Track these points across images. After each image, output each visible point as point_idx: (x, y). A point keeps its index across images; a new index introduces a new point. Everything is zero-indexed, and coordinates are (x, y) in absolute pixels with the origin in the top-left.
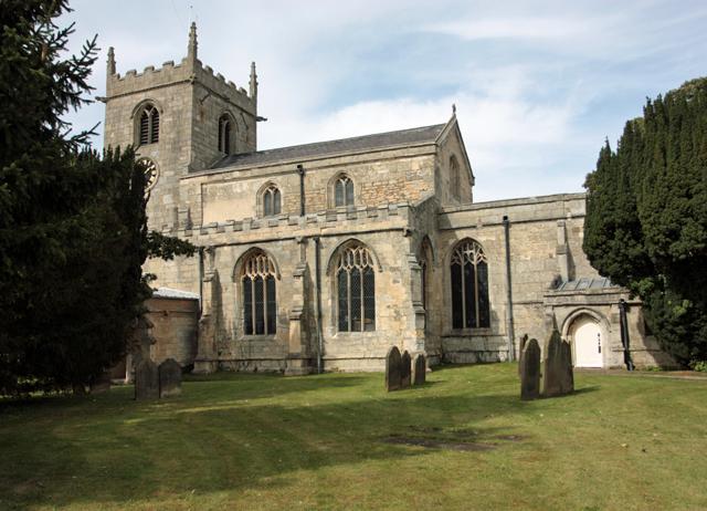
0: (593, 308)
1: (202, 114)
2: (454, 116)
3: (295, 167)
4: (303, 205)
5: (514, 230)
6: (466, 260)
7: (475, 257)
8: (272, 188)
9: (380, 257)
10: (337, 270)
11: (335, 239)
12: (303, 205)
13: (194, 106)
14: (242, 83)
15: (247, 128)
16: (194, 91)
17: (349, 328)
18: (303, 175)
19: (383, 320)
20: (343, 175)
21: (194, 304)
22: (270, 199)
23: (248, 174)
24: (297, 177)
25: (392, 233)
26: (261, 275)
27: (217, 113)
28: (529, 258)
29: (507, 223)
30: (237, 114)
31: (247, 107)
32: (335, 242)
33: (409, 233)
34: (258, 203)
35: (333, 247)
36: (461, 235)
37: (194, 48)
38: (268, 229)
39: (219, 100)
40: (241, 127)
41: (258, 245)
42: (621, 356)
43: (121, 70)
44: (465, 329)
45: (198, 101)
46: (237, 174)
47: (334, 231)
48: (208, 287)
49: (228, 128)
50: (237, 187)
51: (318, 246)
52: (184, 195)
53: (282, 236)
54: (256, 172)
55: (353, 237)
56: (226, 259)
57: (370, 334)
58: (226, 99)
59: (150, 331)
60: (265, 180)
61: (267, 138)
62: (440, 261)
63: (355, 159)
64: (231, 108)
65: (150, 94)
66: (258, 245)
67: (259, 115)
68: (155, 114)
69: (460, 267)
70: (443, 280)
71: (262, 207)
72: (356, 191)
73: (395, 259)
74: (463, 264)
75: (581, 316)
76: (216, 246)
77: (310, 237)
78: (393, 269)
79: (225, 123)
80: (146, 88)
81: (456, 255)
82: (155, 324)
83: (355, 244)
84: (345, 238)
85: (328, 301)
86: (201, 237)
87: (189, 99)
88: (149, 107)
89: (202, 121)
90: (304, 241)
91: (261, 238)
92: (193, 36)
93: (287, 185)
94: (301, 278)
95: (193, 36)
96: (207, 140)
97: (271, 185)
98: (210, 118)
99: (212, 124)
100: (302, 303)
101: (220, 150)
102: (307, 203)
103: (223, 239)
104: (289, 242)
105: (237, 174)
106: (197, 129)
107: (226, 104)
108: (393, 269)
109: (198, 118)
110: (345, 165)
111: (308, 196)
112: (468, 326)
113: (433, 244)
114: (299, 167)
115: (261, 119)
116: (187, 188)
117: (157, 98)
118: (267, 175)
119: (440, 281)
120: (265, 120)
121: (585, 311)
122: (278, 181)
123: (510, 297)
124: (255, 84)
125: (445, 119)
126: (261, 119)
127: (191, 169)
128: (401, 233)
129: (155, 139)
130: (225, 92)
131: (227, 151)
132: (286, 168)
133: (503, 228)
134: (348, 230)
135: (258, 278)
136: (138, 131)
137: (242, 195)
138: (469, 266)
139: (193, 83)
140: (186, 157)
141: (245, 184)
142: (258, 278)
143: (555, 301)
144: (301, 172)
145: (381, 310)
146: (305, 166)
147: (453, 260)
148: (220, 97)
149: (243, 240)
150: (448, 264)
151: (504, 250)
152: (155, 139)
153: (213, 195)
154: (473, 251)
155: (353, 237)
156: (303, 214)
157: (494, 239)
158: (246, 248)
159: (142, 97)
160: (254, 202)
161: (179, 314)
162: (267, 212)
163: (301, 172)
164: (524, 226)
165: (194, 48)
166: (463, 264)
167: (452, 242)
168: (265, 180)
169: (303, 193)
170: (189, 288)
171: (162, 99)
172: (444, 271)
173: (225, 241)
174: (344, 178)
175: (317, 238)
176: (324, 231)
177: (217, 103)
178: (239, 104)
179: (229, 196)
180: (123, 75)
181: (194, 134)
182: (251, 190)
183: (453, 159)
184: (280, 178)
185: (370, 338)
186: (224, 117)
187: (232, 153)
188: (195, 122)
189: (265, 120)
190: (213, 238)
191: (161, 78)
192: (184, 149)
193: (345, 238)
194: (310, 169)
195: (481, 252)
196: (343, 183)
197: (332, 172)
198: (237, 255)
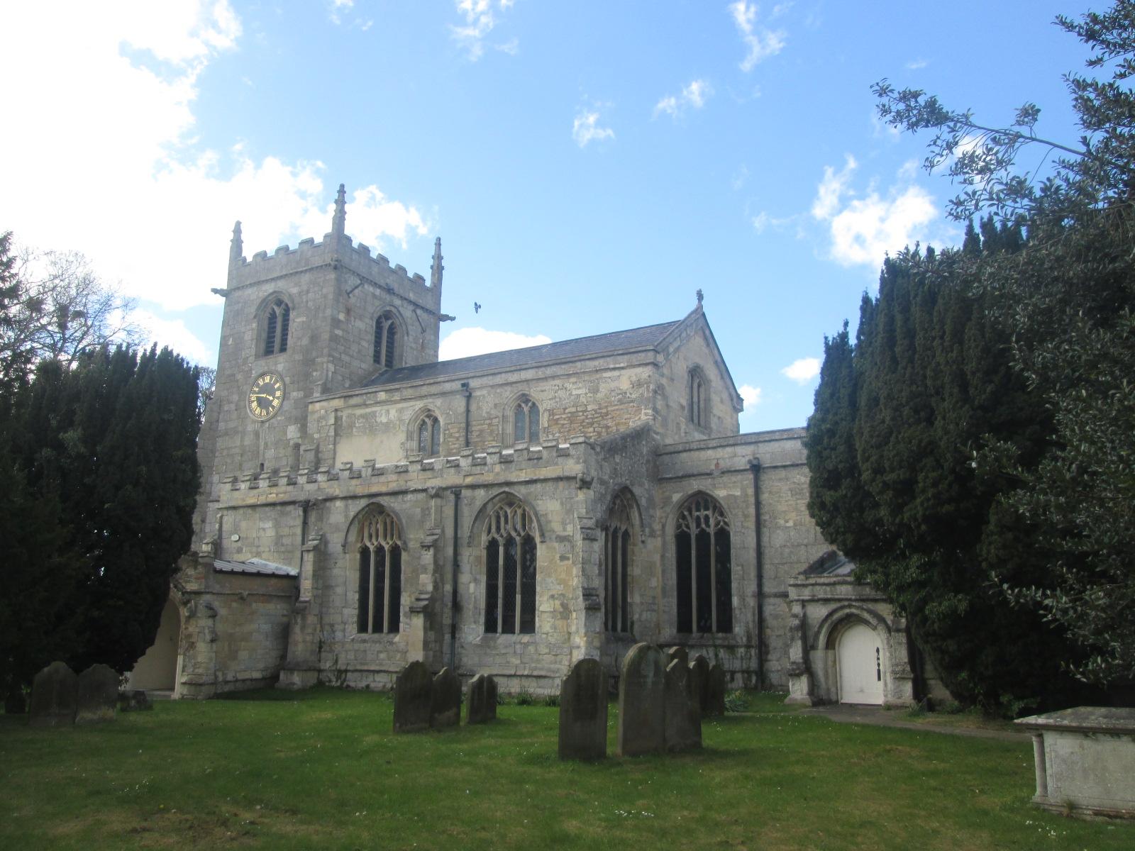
0: (870, 606)
1: (348, 311)
2: (700, 307)
3: (457, 386)
5: (769, 480)
6: (698, 525)
7: (712, 522)
8: (428, 416)
9: (542, 519)
10: (484, 539)
11: (481, 493)
14: (419, 266)
15: (424, 331)
17: (500, 629)
18: (469, 397)
19: (545, 616)
20: (525, 398)
21: (295, 579)
23: (397, 396)
25: (561, 484)
26: (383, 543)
27: (374, 309)
28: (791, 524)
29: (757, 468)
30: (407, 312)
31: (428, 302)
33: (585, 484)
34: (409, 437)
35: (478, 504)
36: (695, 485)
38: (394, 477)
39: (378, 292)
40: (414, 330)
41: (374, 500)
42: (908, 688)
43: (249, 253)
44: (695, 633)
45: (342, 294)
48: (309, 558)
51: (458, 496)
52: (312, 427)
53: (413, 485)
54: (408, 393)
55: (507, 489)
56: (339, 514)
57: (526, 638)
58: (389, 291)
60: (419, 405)
61: (455, 344)
62: (657, 527)
63: (540, 373)
64: (397, 302)
65: (281, 285)
67: (443, 312)
69: (689, 535)
70: (663, 556)
71: (414, 444)
72: (544, 420)
73: (564, 524)
74: (694, 531)
75: (849, 616)
76: (326, 500)
78: (561, 539)
79: (386, 325)
80: (275, 275)
81: (684, 517)
83: (510, 500)
84: (496, 491)
85: (474, 589)
87: (329, 290)
88: (279, 302)
89: (348, 321)
90: (439, 493)
91: (384, 489)
94: (432, 551)
96: (355, 348)
97: (429, 413)
98: (361, 318)
99: (364, 326)
100: (430, 588)
101: (377, 359)
103: (335, 489)
104: (421, 496)
107: (388, 297)
108: (561, 539)
109: (342, 317)
111: (475, 428)
112: (720, 629)
113: (643, 502)
114: (463, 385)
115: (446, 318)
116: (316, 416)
118: (421, 397)
119: (657, 558)
121: (853, 610)
122: (437, 405)
123: (760, 585)
124: (438, 269)
125: (677, 310)
126: (446, 318)
128: (574, 485)
129: (283, 349)
130: (392, 281)
131: (389, 363)
133: (751, 476)
134: (501, 479)
135: (380, 550)
136: (264, 335)
137: (388, 427)
138: (703, 536)
139: (335, 268)
142: (380, 550)
143: (806, 594)
145: (544, 604)
146: (473, 383)
147: (679, 526)
148: (380, 287)
149: (360, 491)
150: (671, 531)
151: (752, 511)
152: (283, 349)
153: (351, 426)
154: (709, 513)
155: (507, 489)
157: (738, 493)
158: (363, 502)
159: (269, 288)
160: (402, 437)
164: (783, 473)
166: (694, 531)
167: (676, 497)
168: (419, 405)
169: (468, 424)
170: (288, 561)
171: (294, 290)
172: (664, 544)
173: (337, 492)
174: (527, 401)
175: (456, 491)
176: (469, 480)
177: (374, 296)
178: (412, 296)
179: (372, 428)
180: (249, 259)
182: (401, 420)
183: (695, 373)
184: (439, 402)
185: (526, 645)
186: (387, 315)
187: (397, 365)
189: (453, 319)
190: (324, 486)
193: (496, 491)
194: (481, 388)
195: (722, 514)
196: (526, 409)
197: (509, 394)
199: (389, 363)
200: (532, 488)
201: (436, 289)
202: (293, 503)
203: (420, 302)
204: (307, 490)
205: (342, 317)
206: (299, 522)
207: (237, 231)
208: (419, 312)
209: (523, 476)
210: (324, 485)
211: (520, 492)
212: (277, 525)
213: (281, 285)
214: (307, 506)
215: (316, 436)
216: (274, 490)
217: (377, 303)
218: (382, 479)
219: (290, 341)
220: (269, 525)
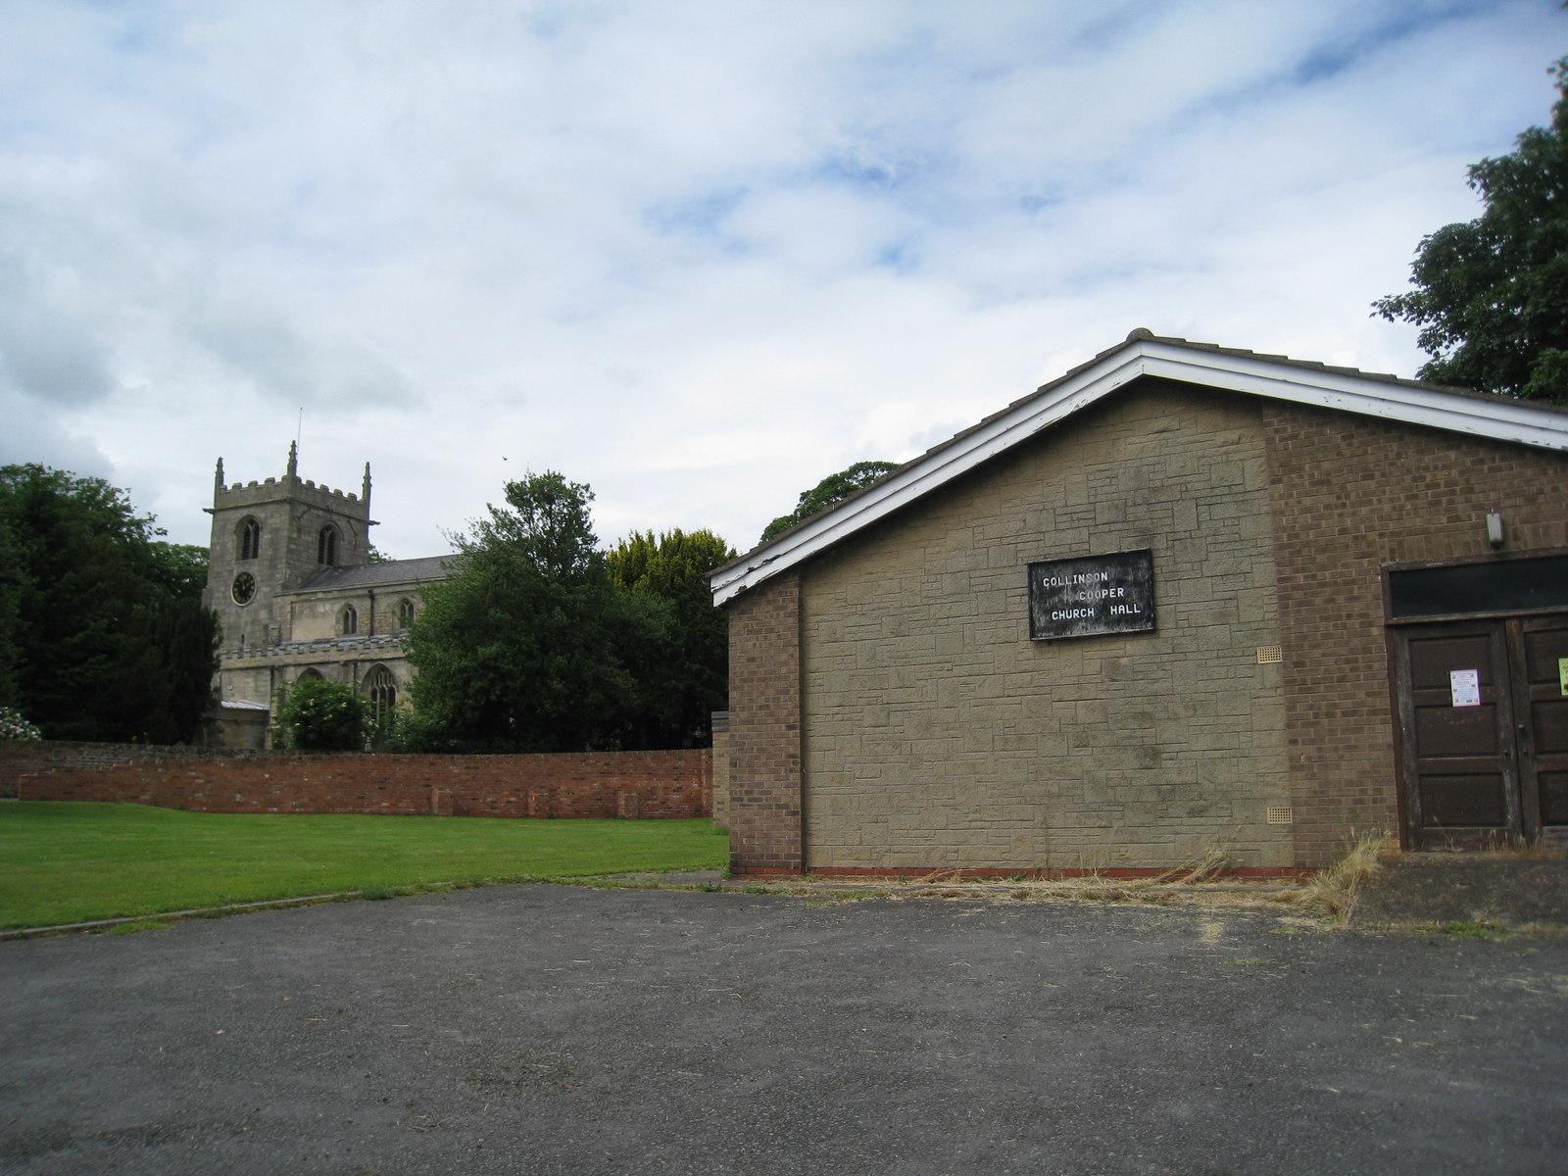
1: (299, 531)
3: (366, 592)
4: (372, 627)
8: (350, 609)
12: (372, 627)
13: (291, 525)
15: (356, 535)
16: (292, 510)
21: (265, 713)
22: (349, 621)
23: (330, 596)
24: (367, 603)
27: (318, 525)
30: (342, 523)
32: (368, 666)
34: (338, 622)
35: (367, 669)
37: (293, 465)
38: (323, 654)
39: (321, 513)
40: (348, 536)
41: (312, 666)
43: (229, 483)
45: (295, 519)
46: (320, 595)
47: (368, 657)
49: (332, 538)
50: (321, 608)
51: (356, 666)
52: (276, 612)
53: (332, 659)
56: (291, 675)
58: (328, 511)
59: (221, 735)
64: (335, 517)
65: (252, 511)
66: (312, 666)
68: (257, 530)
71: (341, 627)
76: (284, 666)
77: (349, 661)
79: (328, 534)
80: (249, 503)
82: (227, 730)
83: (384, 669)
86: (273, 658)
87: (286, 517)
90: (346, 663)
92: (293, 454)
93: (362, 607)
95: (293, 454)
97: (350, 607)
98: (309, 533)
99: (311, 538)
101: (321, 560)
102: (376, 625)
103: (289, 660)
104: (336, 665)
105: (320, 595)
106: (293, 547)
109: (295, 535)
110: (407, 592)
111: (377, 618)
114: (370, 591)
117: (260, 514)
118: (345, 598)
120: (378, 524)
122: (355, 603)
124: (367, 487)
127: (285, 587)
129: (255, 556)
131: (330, 562)
132: (360, 592)
136: (242, 545)
137: (324, 615)
139: (290, 503)
140: (283, 573)
141: (328, 606)
144: (372, 597)
146: (376, 591)
148: (322, 509)
152: (255, 556)
153: (302, 612)
156: (372, 634)
159: (245, 512)
161: (252, 723)
162: (346, 632)
163: (372, 597)
165: (293, 465)
168: (343, 602)
169: (372, 615)
171: (262, 515)
174: (407, 604)
175: (355, 662)
179: (314, 615)
180: (229, 488)
181: (290, 551)
182: (332, 611)
184: (355, 601)
186: (328, 528)
188: (290, 540)
189: (378, 524)
191: (263, 494)
192: (279, 566)
196: (407, 608)
197: (396, 599)
198: (299, 674)
199: (330, 562)
200: (393, 663)
201: (366, 504)
202: (265, 667)
203: (354, 514)
204: (272, 659)
205: (295, 535)
206: (269, 678)
207: (220, 465)
208: (352, 522)
209: (389, 656)
210: (283, 657)
211: (387, 664)
212: (256, 680)
213: (252, 511)
214: (273, 669)
215: (279, 619)
216: (253, 659)
217: (320, 521)
218: (316, 654)
219: (260, 551)
220: (250, 680)
